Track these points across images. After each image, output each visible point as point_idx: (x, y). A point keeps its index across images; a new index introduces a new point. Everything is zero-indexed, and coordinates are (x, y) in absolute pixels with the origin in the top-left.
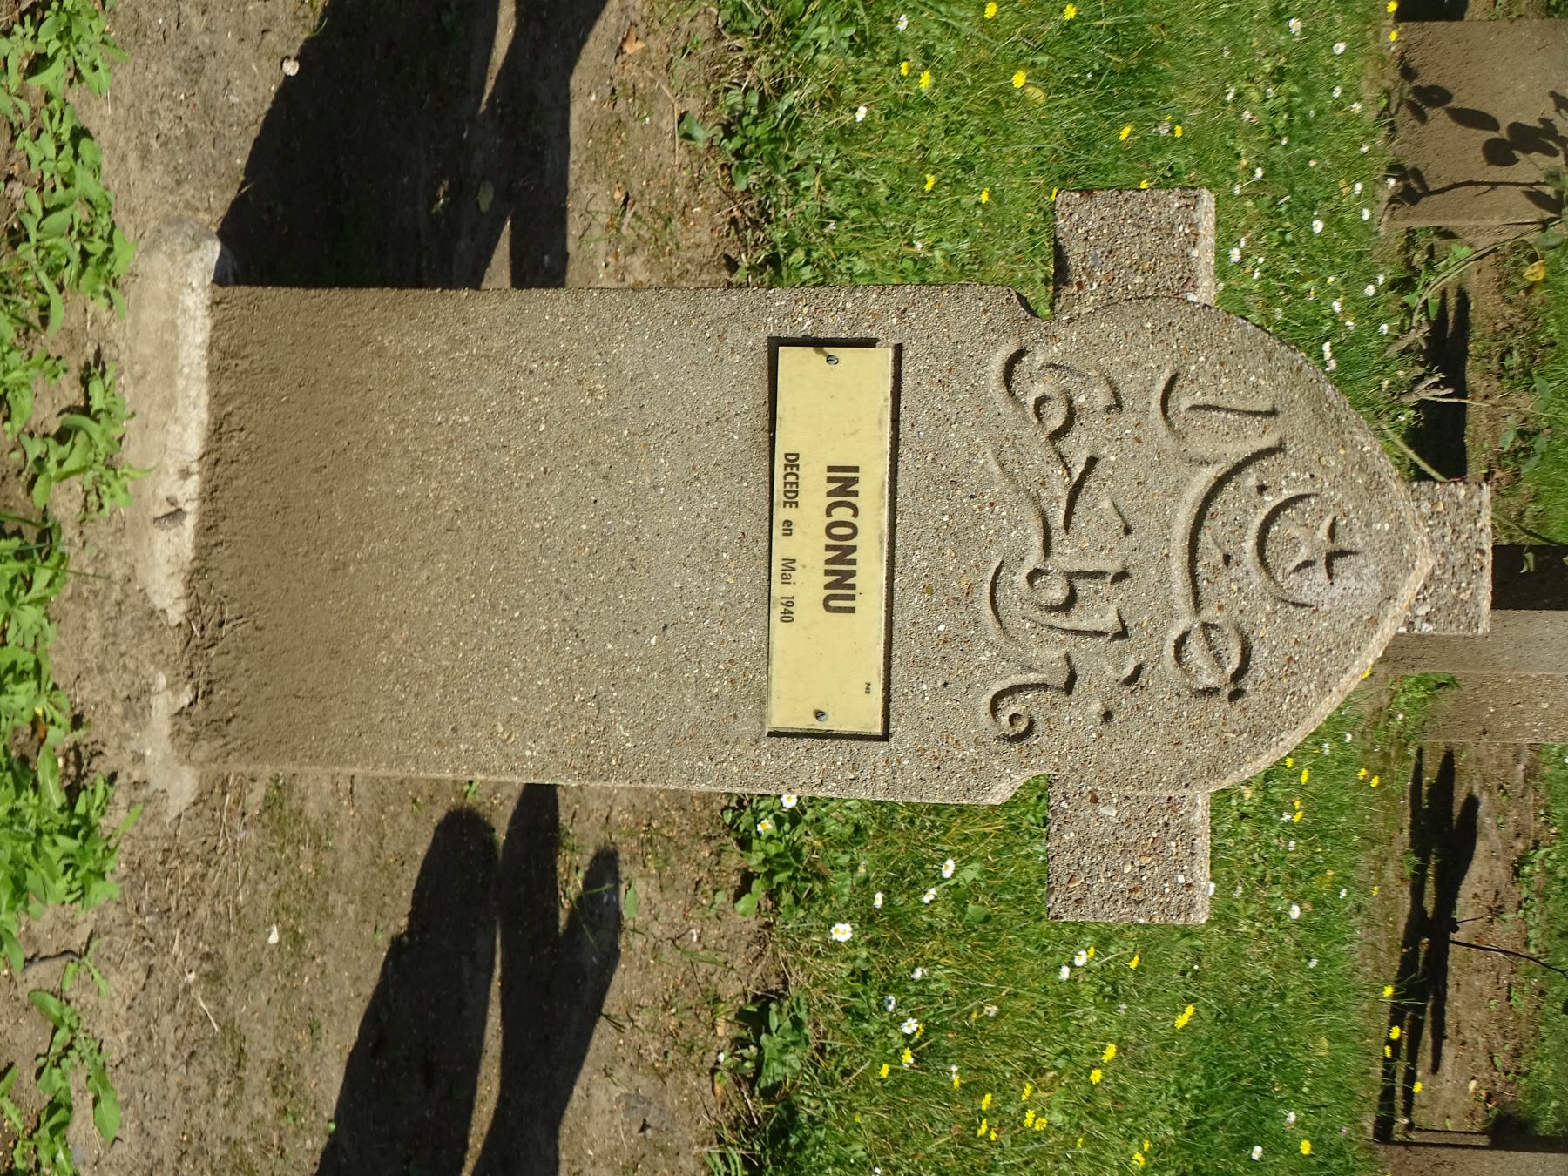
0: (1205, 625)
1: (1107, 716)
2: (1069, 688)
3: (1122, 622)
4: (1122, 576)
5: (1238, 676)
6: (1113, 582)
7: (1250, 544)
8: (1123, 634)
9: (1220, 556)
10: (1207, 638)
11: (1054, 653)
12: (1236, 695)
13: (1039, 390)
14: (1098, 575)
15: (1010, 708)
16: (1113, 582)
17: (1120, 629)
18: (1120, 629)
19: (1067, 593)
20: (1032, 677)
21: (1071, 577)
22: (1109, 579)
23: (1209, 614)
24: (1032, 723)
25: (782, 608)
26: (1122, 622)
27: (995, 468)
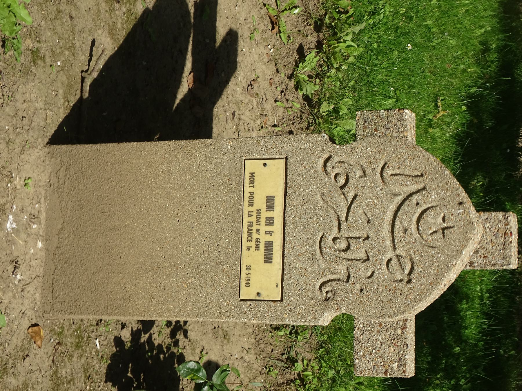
0: (397, 256)
1: (362, 290)
2: (348, 281)
3: (368, 256)
4: (368, 238)
7: (414, 226)
8: (368, 260)
10: (399, 260)
13: (337, 171)
15: (326, 289)
17: (366, 258)
18: (366, 258)
20: (334, 277)
21: (347, 238)
22: (362, 239)
26: (368, 256)
27: (321, 203)
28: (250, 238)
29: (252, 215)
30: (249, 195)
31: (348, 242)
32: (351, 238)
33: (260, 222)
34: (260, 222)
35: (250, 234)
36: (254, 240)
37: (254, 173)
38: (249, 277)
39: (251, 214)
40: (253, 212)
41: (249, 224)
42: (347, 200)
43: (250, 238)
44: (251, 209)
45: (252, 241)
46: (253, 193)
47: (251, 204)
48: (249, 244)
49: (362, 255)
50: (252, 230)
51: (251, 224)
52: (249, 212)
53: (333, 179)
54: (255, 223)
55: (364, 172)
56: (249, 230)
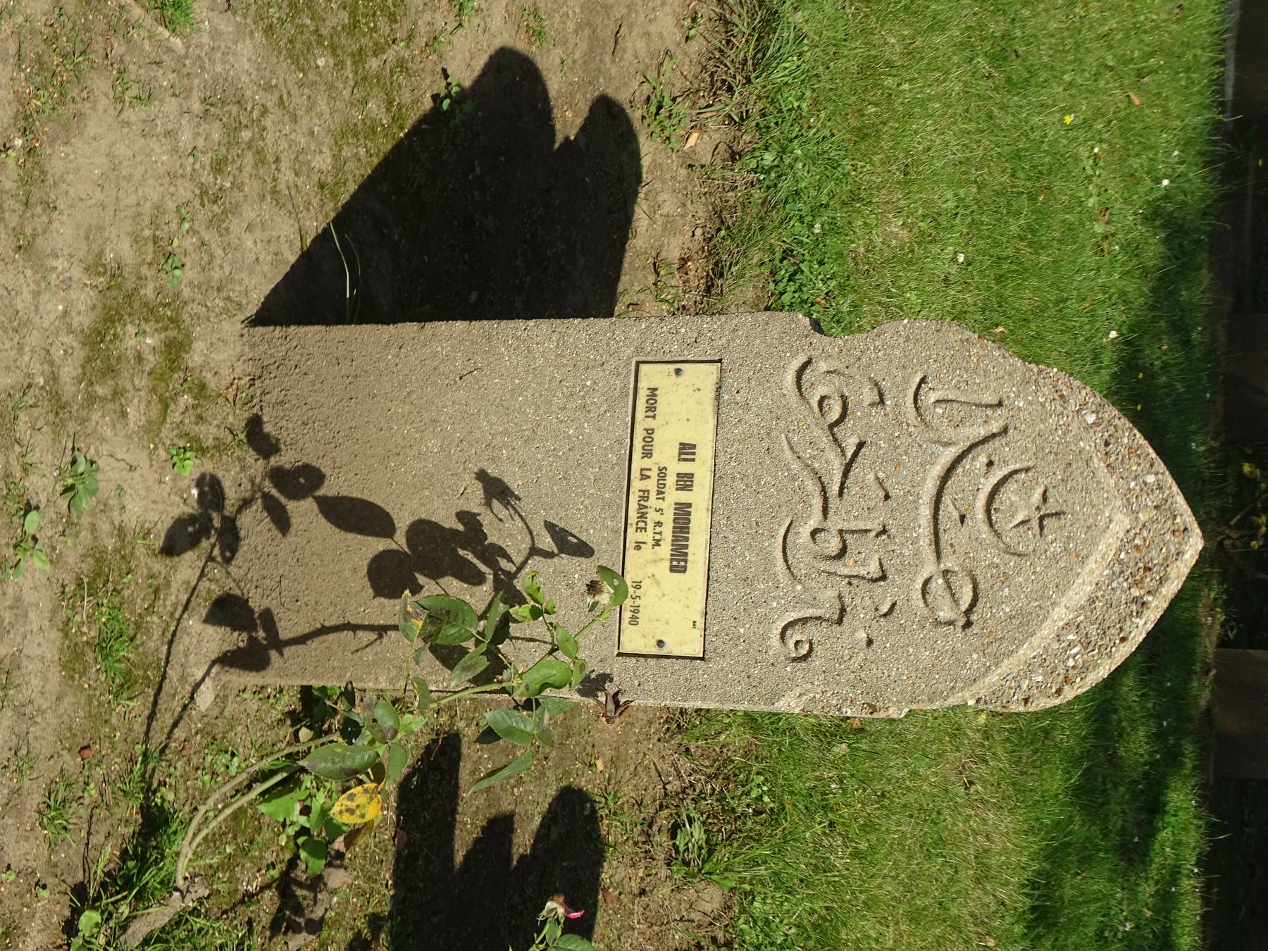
0: (946, 573)
1: (870, 642)
2: (840, 622)
5: (968, 612)
6: (877, 536)
7: (980, 515)
8: (883, 577)
9: (956, 515)
10: (947, 582)
11: (831, 594)
12: (968, 624)
14: (867, 531)
16: (877, 536)
19: (840, 546)
22: (873, 534)
23: (948, 563)
24: (811, 649)
25: (630, 614)
26: (883, 571)
28: (641, 525)
29: (649, 477)
30: (645, 433)
31: (844, 542)
32: (847, 532)
33: (663, 493)
34: (663, 493)
35: (642, 516)
36: (650, 526)
37: (657, 389)
38: (638, 602)
39: (647, 473)
40: (650, 470)
41: (641, 494)
42: (843, 452)
43: (641, 525)
44: (647, 463)
45: (645, 529)
46: (653, 430)
47: (647, 454)
48: (641, 536)
49: (873, 569)
50: (646, 507)
51: (645, 495)
52: (642, 470)
53: (816, 409)
54: (653, 495)
55: (881, 395)
56: (641, 507)
